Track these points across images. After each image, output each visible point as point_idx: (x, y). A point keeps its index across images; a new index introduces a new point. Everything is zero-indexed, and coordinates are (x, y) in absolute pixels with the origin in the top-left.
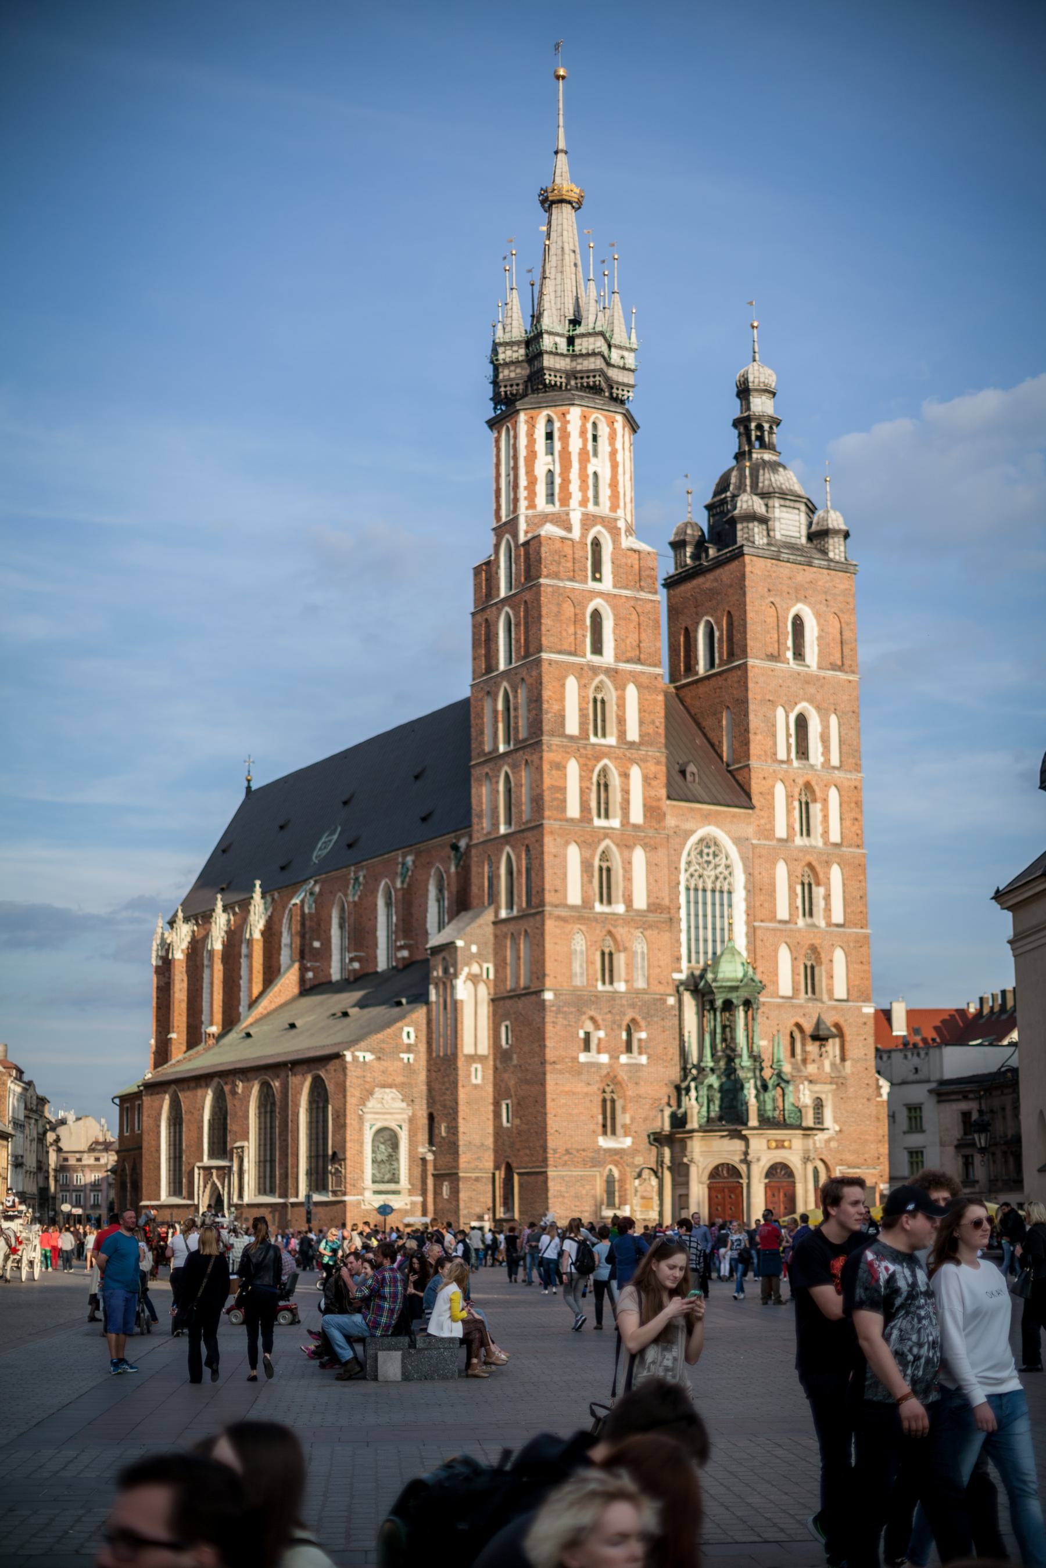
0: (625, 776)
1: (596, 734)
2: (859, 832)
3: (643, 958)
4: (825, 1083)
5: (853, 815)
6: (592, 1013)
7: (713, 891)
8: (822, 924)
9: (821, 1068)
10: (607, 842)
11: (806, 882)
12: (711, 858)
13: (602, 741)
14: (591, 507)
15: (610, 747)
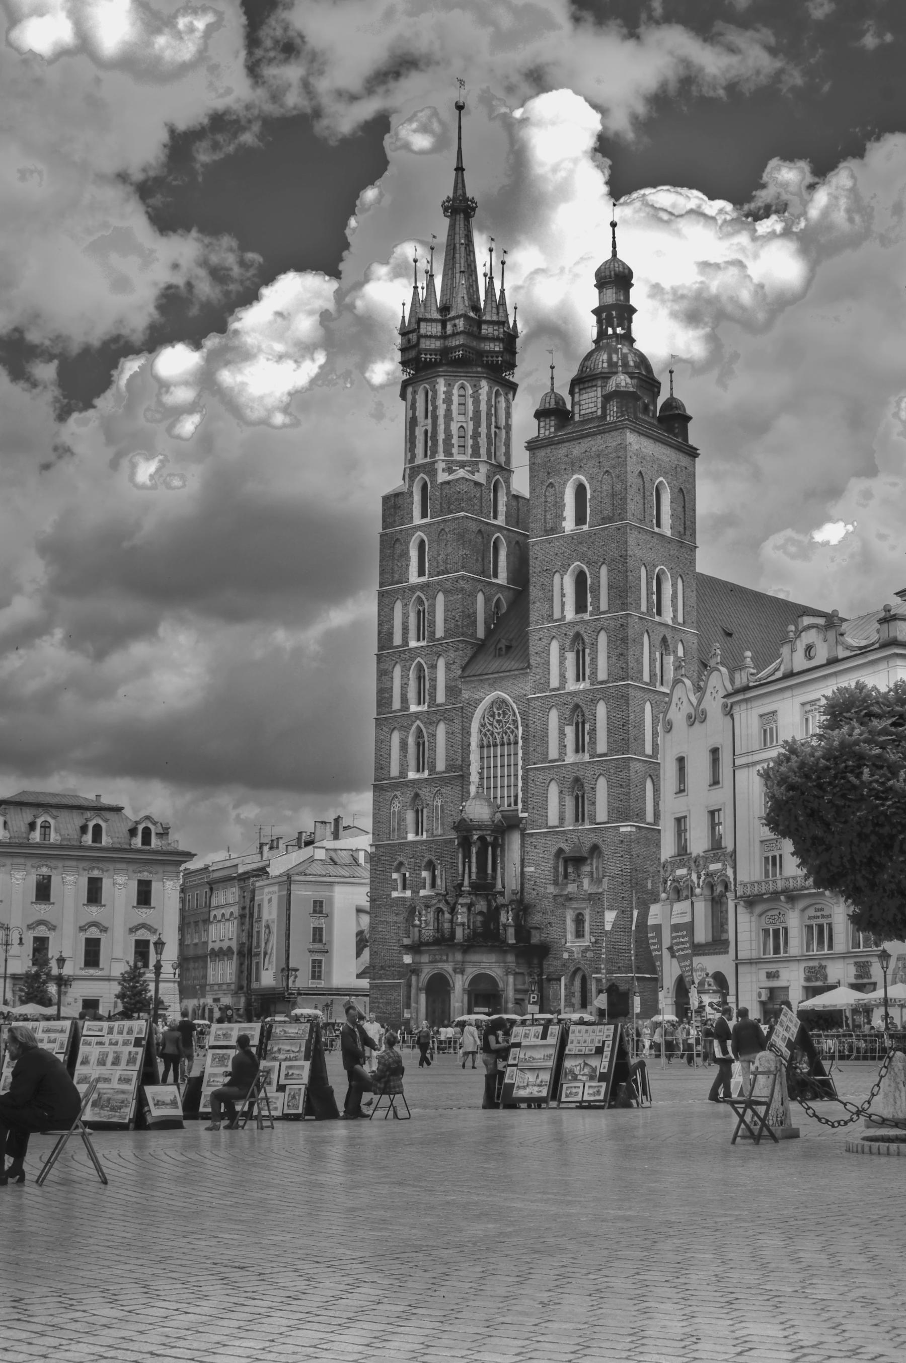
0: (434, 667)
1: (419, 640)
2: (624, 665)
3: (442, 811)
4: (584, 900)
5: (619, 651)
6: (401, 859)
7: (502, 745)
8: (586, 758)
9: (580, 886)
10: (418, 722)
11: (580, 721)
12: (501, 718)
13: (423, 643)
14: (420, 460)
15: (422, 647)
